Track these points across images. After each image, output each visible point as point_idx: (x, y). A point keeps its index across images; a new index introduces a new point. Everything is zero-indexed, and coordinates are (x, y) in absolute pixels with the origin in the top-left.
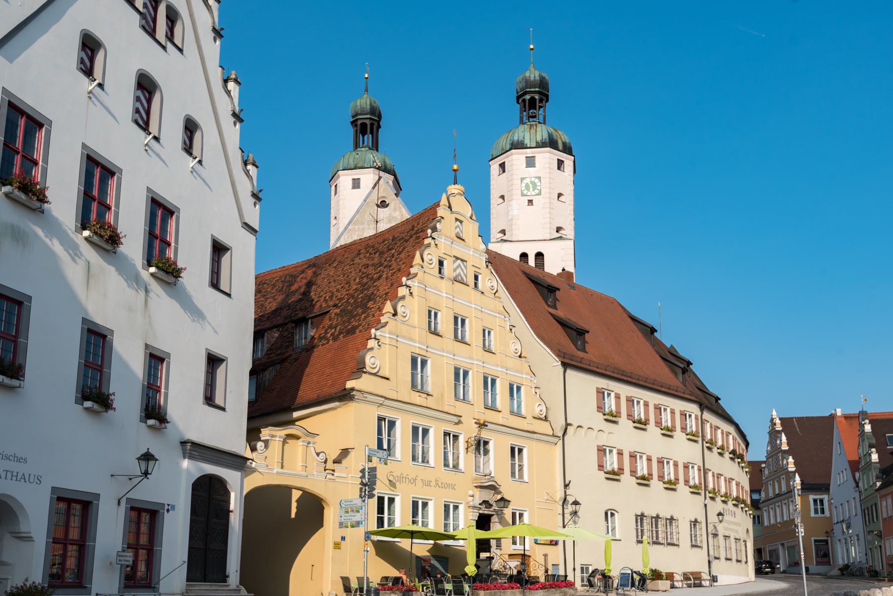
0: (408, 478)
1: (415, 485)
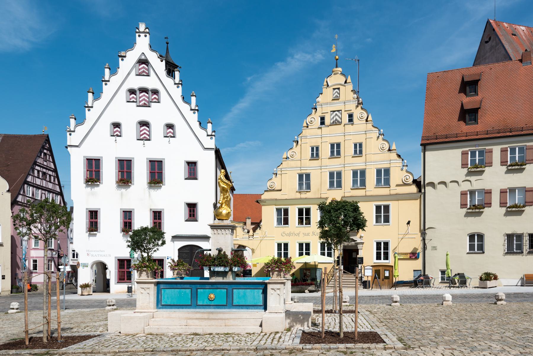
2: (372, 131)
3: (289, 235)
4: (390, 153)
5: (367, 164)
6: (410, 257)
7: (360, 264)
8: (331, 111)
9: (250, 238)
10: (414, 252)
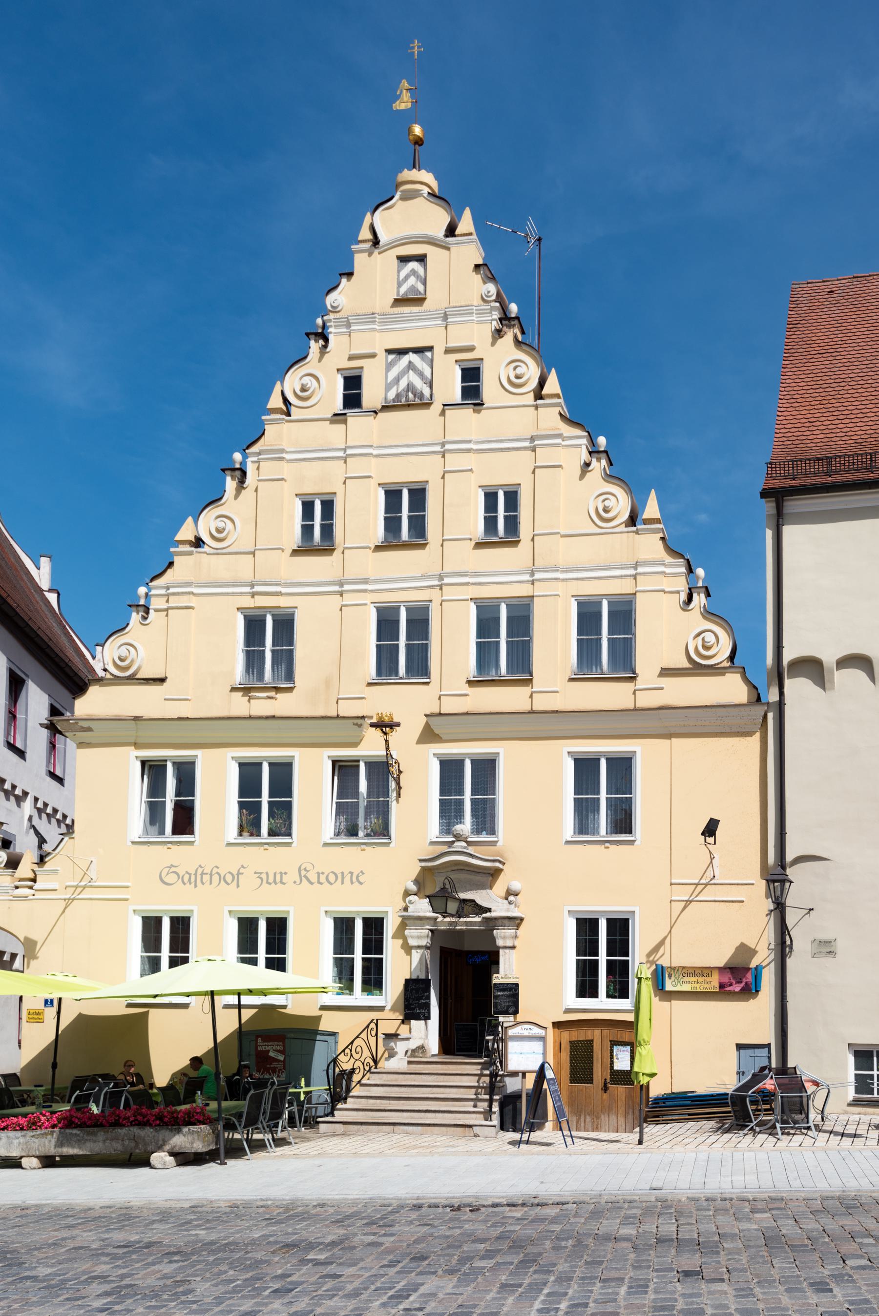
0: (217, 873)
1: (238, 886)
2: (559, 436)
3: (195, 878)
4: (637, 532)
6: (722, 986)
7: (506, 1013)
8: (389, 351)
10: (738, 963)
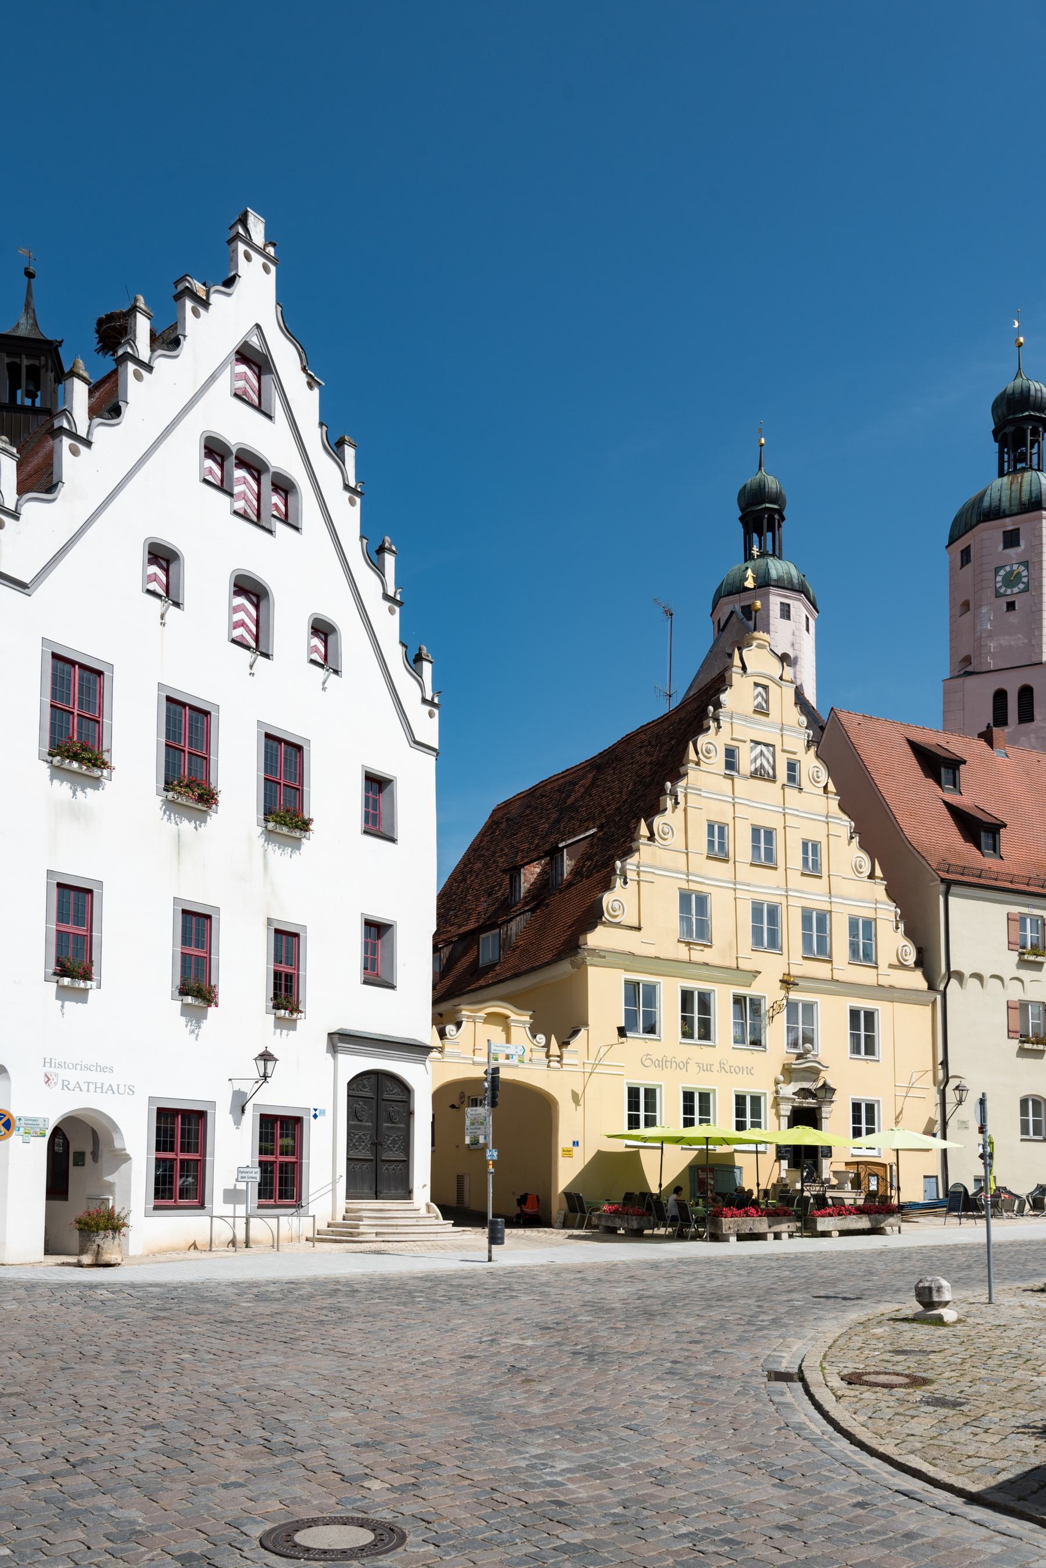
3: (662, 1064)
5: (833, 899)
8: (752, 741)
9: (552, 1064)
